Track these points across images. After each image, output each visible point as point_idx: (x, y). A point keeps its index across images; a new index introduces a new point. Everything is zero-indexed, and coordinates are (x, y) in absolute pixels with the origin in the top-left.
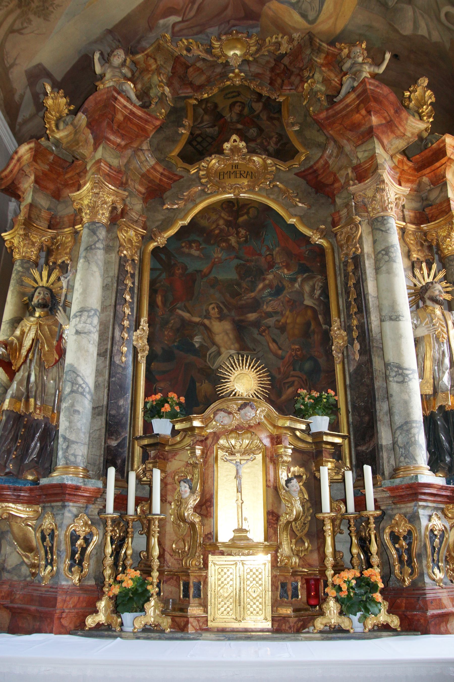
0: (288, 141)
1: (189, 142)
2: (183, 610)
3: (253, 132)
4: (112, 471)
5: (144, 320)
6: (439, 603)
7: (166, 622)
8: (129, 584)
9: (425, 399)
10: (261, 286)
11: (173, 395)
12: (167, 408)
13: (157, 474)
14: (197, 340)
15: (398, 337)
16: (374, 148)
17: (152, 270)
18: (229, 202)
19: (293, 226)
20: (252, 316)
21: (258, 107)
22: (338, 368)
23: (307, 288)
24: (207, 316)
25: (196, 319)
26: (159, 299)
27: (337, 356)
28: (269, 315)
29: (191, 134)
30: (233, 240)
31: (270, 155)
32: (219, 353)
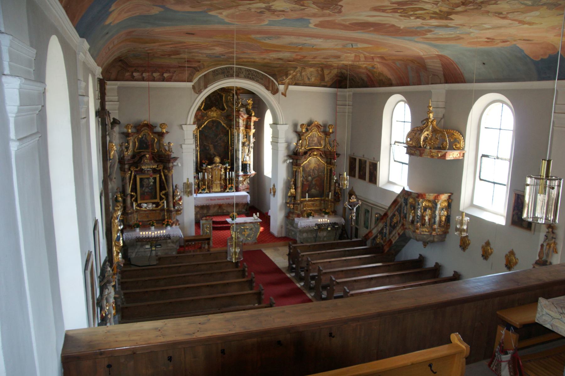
0: (224, 106)
1: (204, 105)
2: (210, 190)
3: (217, 103)
4: (200, 174)
5: (199, 146)
6: (240, 189)
7: (208, 192)
8: (204, 188)
9: (242, 162)
10: (218, 138)
11: (206, 161)
12: (206, 163)
13: (206, 174)
14: (207, 148)
15: (239, 154)
16: (239, 120)
17: (199, 135)
18: (213, 121)
19: (223, 126)
20: (216, 144)
21: (218, 96)
22: (230, 153)
23: (225, 139)
24: (209, 144)
25: (207, 144)
26: (201, 141)
27: (230, 151)
28: (219, 143)
29: (205, 103)
30: (213, 129)
31: (220, 109)
32: (211, 150)
